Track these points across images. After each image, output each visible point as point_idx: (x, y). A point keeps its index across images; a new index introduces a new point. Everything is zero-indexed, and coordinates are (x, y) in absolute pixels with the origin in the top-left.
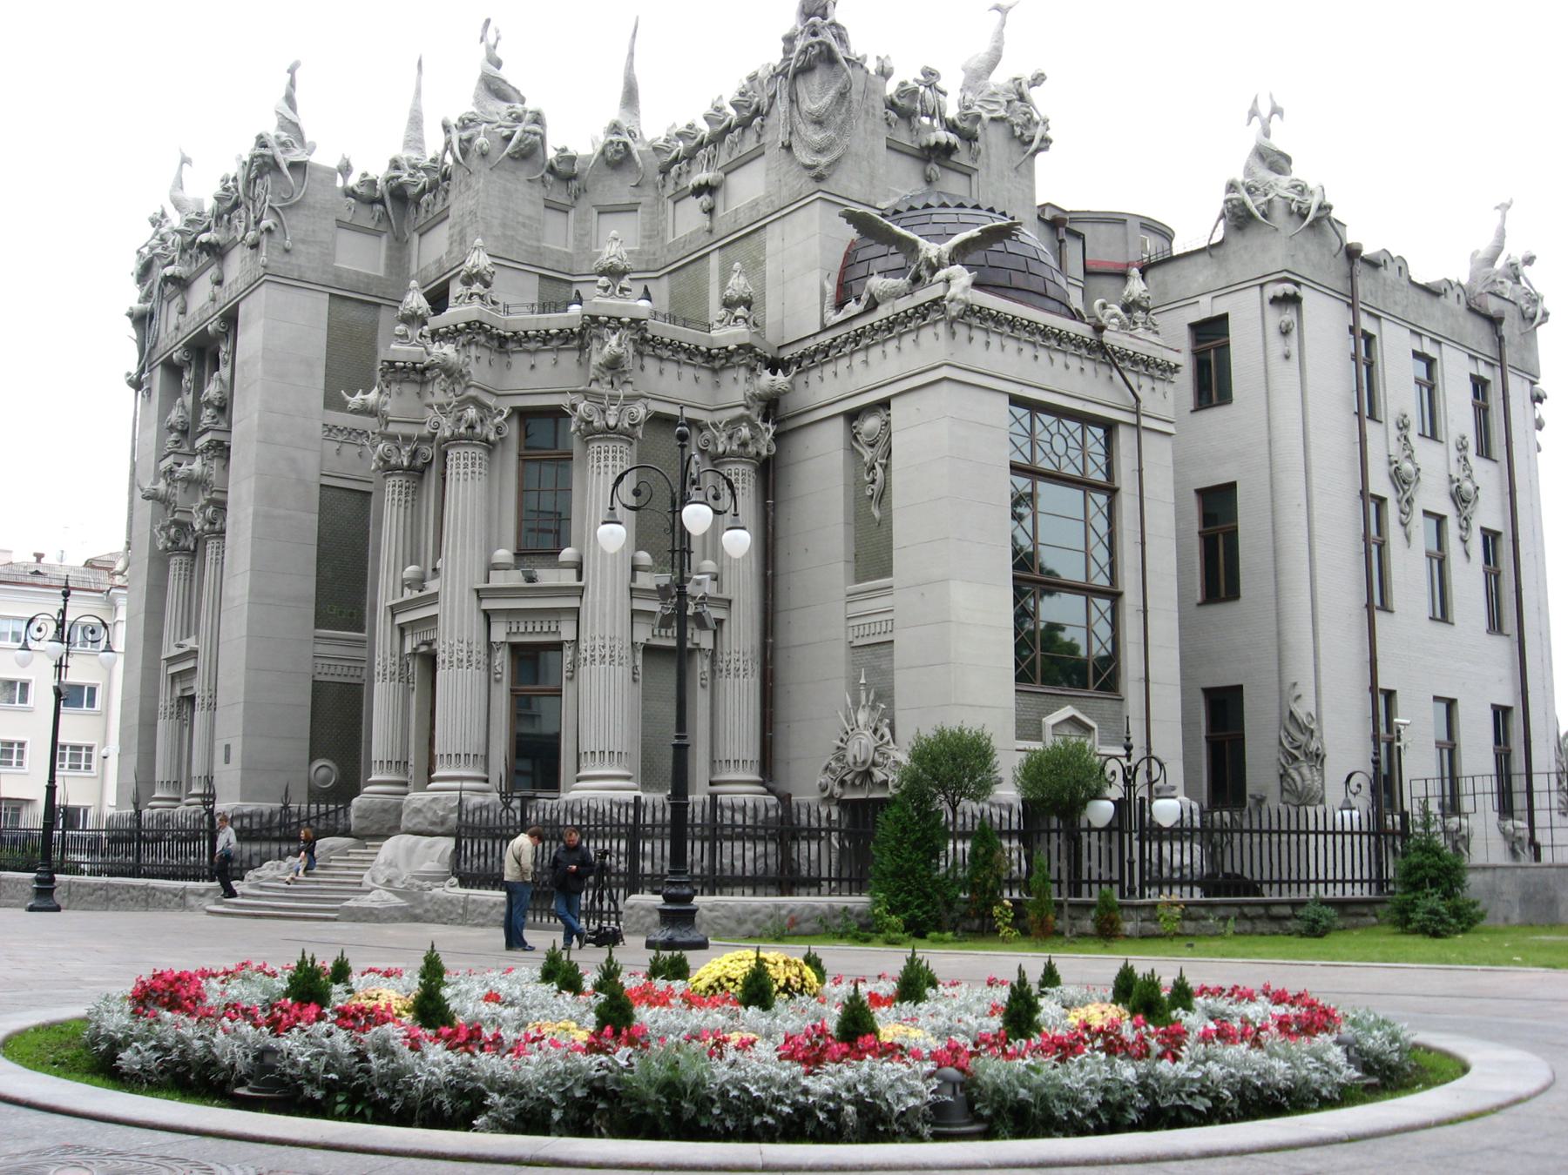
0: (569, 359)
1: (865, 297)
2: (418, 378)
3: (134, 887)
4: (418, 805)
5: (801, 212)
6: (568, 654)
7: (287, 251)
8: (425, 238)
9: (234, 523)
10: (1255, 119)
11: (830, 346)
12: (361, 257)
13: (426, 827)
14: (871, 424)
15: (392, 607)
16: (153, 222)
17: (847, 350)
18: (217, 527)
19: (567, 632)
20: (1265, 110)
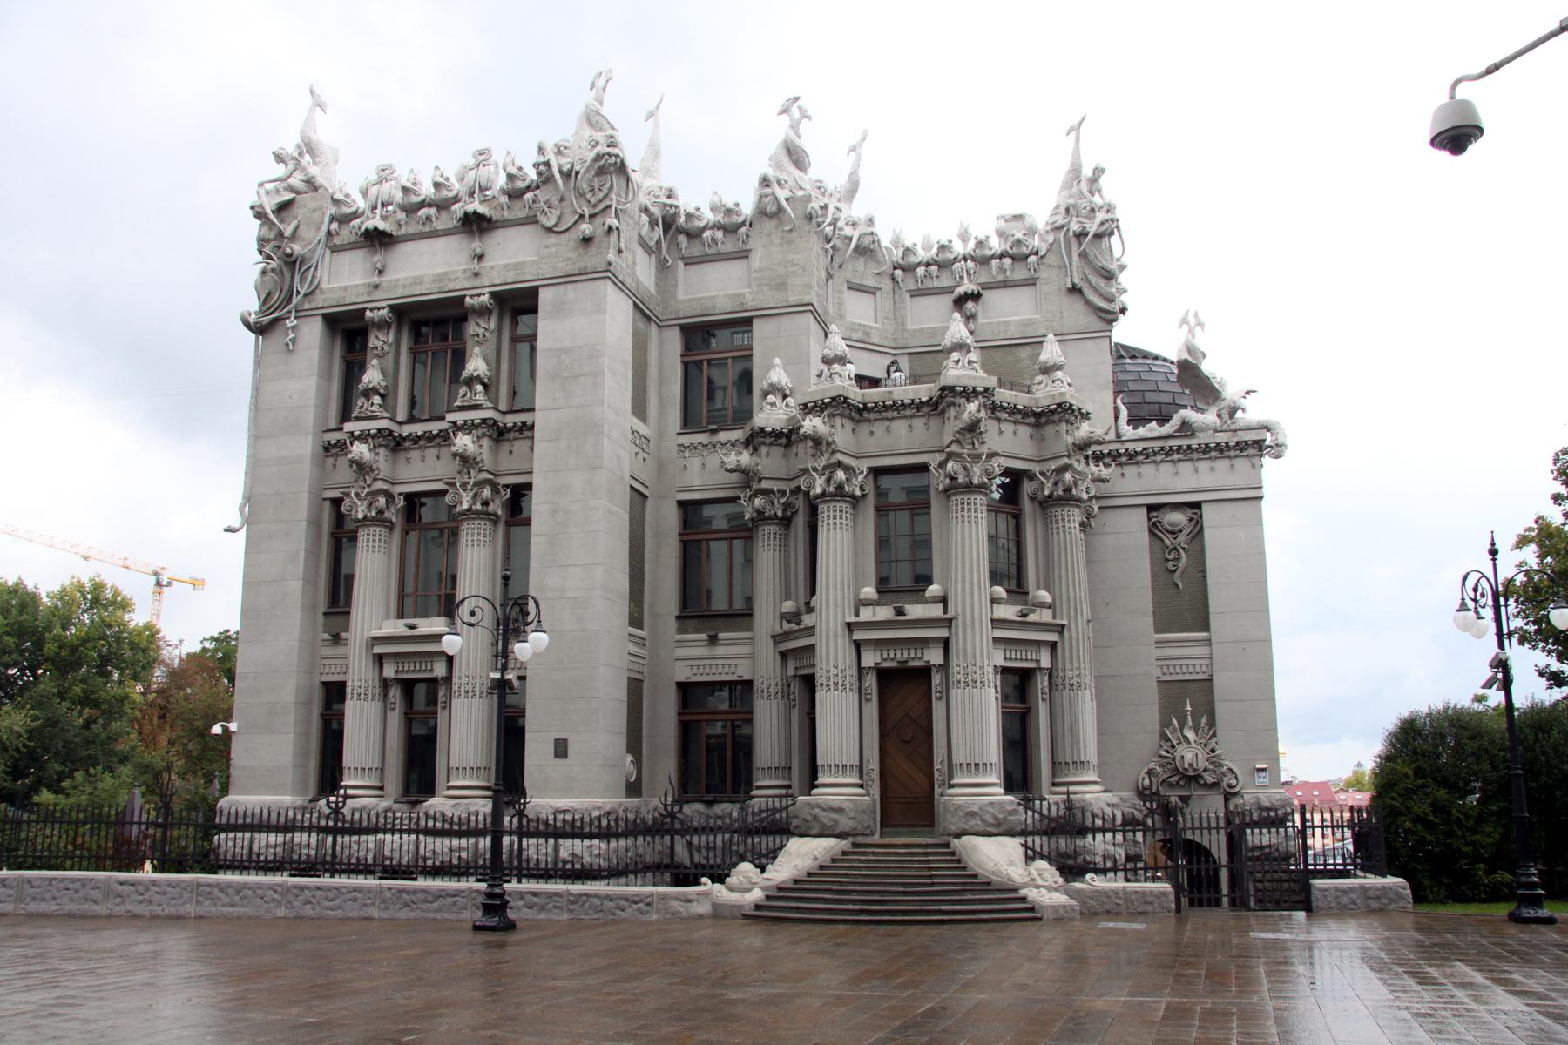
0: (1024, 431)
1: (1175, 422)
2: (857, 417)
3: (535, 894)
4: (975, 808)
5: (1089, 344)
6: (1042, 682)
7: (620, 252)
8: (691, 268)
9: (554, 512)
10: (1185, 327)
11: (1137, 453)
12: (643, 271)
13: (981, 828)
14: (1178, 518)
15: (849, 625)
16: (279, 158)
17: (1159, 458)
18: (491, 508)
19: (1045, 662)
20: (1192, 320)
